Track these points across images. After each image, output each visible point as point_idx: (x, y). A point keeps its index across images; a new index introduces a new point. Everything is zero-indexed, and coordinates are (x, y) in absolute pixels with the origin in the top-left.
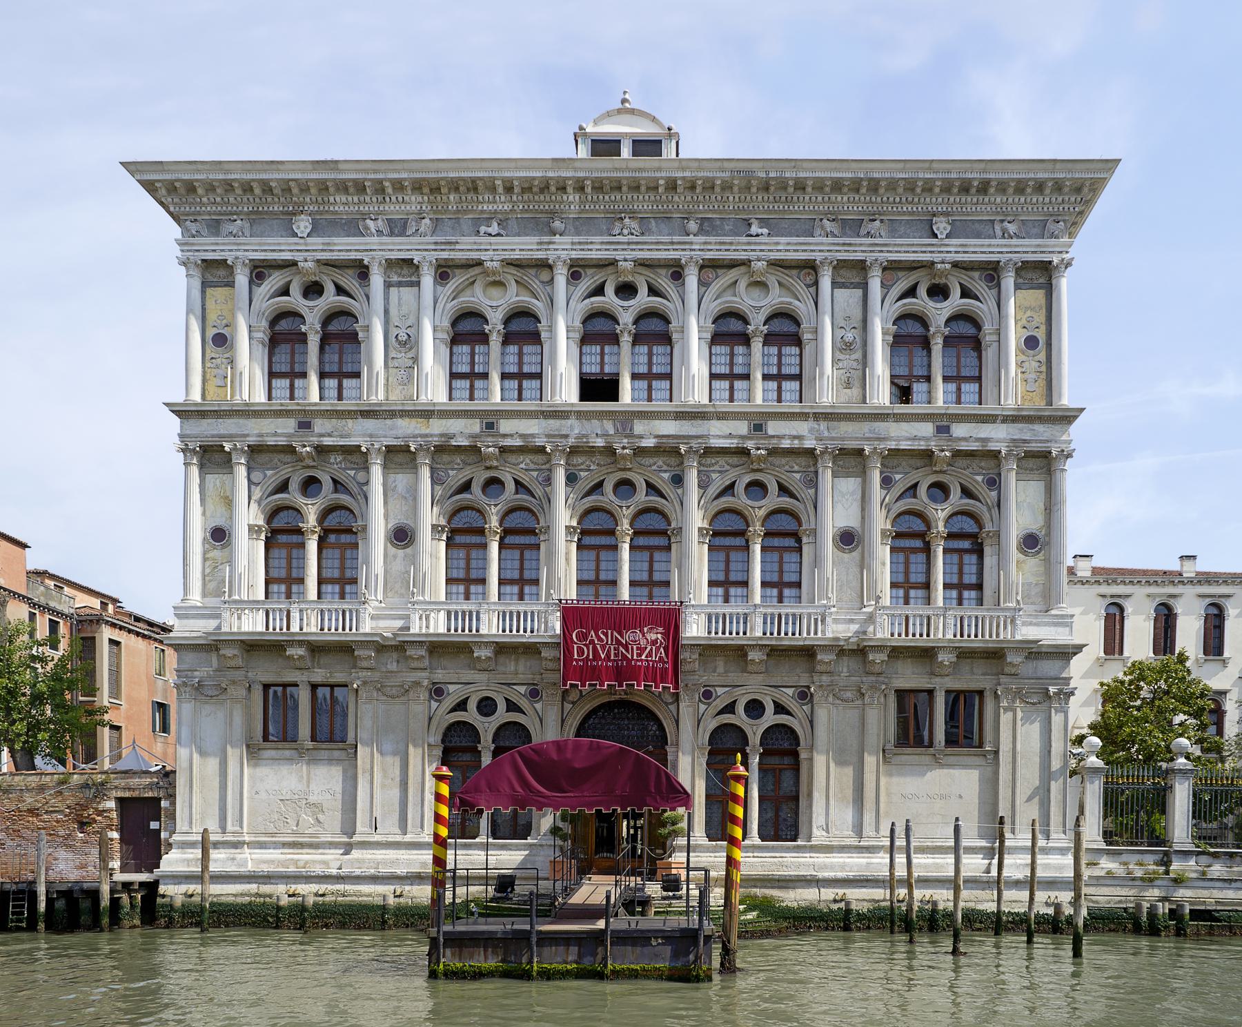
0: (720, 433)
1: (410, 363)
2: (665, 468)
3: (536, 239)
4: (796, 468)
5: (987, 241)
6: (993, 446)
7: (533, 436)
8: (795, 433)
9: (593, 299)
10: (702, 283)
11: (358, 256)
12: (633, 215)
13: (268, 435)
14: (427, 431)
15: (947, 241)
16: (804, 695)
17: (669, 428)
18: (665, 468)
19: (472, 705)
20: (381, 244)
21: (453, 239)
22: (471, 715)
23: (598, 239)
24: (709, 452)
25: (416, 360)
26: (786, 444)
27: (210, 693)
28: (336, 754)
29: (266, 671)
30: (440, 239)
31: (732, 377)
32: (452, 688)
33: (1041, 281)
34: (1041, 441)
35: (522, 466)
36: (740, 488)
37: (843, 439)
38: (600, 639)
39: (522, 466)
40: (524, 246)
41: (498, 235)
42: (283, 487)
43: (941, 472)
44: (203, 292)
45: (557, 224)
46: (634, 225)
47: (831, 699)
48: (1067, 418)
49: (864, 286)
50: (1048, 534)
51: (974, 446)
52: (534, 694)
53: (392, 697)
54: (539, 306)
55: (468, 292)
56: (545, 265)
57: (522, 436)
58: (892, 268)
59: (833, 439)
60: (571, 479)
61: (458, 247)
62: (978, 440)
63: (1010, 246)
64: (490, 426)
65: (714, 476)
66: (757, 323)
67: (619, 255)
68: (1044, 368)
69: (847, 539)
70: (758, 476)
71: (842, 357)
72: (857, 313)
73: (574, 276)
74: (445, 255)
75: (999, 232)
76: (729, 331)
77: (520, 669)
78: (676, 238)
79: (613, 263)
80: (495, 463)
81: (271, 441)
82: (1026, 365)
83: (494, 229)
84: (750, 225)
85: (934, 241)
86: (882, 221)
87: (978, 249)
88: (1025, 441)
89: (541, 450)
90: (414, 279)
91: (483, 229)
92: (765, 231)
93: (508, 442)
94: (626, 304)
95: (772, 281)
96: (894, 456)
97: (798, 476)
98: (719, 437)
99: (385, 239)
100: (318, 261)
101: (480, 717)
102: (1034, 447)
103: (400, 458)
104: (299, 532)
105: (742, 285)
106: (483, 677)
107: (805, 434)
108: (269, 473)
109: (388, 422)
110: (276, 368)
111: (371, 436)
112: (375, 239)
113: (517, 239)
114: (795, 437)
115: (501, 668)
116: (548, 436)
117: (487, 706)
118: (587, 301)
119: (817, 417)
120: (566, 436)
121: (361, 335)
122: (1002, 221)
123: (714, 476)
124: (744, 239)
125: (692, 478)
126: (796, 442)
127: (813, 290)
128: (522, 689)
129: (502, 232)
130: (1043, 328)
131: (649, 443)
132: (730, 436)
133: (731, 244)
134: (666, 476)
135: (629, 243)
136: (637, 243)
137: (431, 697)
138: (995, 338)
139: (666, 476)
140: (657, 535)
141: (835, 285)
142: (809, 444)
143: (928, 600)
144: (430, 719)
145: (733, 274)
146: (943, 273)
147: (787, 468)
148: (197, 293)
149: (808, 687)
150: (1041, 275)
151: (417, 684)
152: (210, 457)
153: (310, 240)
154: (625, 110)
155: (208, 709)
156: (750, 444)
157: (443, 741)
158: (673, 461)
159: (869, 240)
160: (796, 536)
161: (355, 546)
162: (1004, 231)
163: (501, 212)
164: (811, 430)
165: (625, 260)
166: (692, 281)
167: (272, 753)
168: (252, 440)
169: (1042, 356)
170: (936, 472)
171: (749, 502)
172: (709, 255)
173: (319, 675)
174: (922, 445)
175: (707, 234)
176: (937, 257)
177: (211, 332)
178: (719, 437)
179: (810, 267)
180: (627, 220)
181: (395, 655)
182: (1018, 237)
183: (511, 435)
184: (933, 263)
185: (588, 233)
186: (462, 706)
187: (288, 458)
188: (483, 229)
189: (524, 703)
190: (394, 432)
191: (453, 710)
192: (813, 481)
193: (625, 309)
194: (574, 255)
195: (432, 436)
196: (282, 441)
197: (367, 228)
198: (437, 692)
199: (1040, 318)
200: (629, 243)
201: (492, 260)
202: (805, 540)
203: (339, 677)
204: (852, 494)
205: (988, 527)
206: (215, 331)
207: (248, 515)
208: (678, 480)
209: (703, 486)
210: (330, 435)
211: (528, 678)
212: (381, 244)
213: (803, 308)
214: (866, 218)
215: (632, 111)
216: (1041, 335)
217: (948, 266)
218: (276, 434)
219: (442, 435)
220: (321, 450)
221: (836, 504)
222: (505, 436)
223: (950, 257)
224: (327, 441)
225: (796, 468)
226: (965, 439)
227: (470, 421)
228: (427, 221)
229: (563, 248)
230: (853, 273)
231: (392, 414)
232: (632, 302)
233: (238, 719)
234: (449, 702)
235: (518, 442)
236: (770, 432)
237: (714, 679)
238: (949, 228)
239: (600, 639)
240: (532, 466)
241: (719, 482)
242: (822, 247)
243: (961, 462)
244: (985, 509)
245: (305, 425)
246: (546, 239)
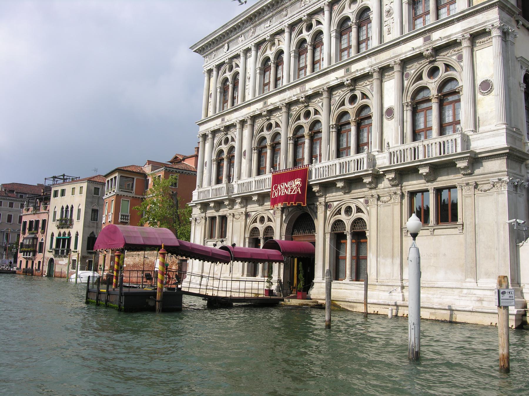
4: (368, 83)
6: (453, 38)
7: (276, 103)
8: (362, 67)
16: (367, 202)
34: (480, 24)
38: (281, 187)
51: (444, 42)
62: (445, 38)
88: (471, 28)
114: (361, 70)
116: (280, 101)
120: (285, 99)
126: (362, 71)
147: (364, 85)
168: (212, 129)
174: (417, 52)
219: (253, 112)
226: (438, 40)
239: (281, 187)
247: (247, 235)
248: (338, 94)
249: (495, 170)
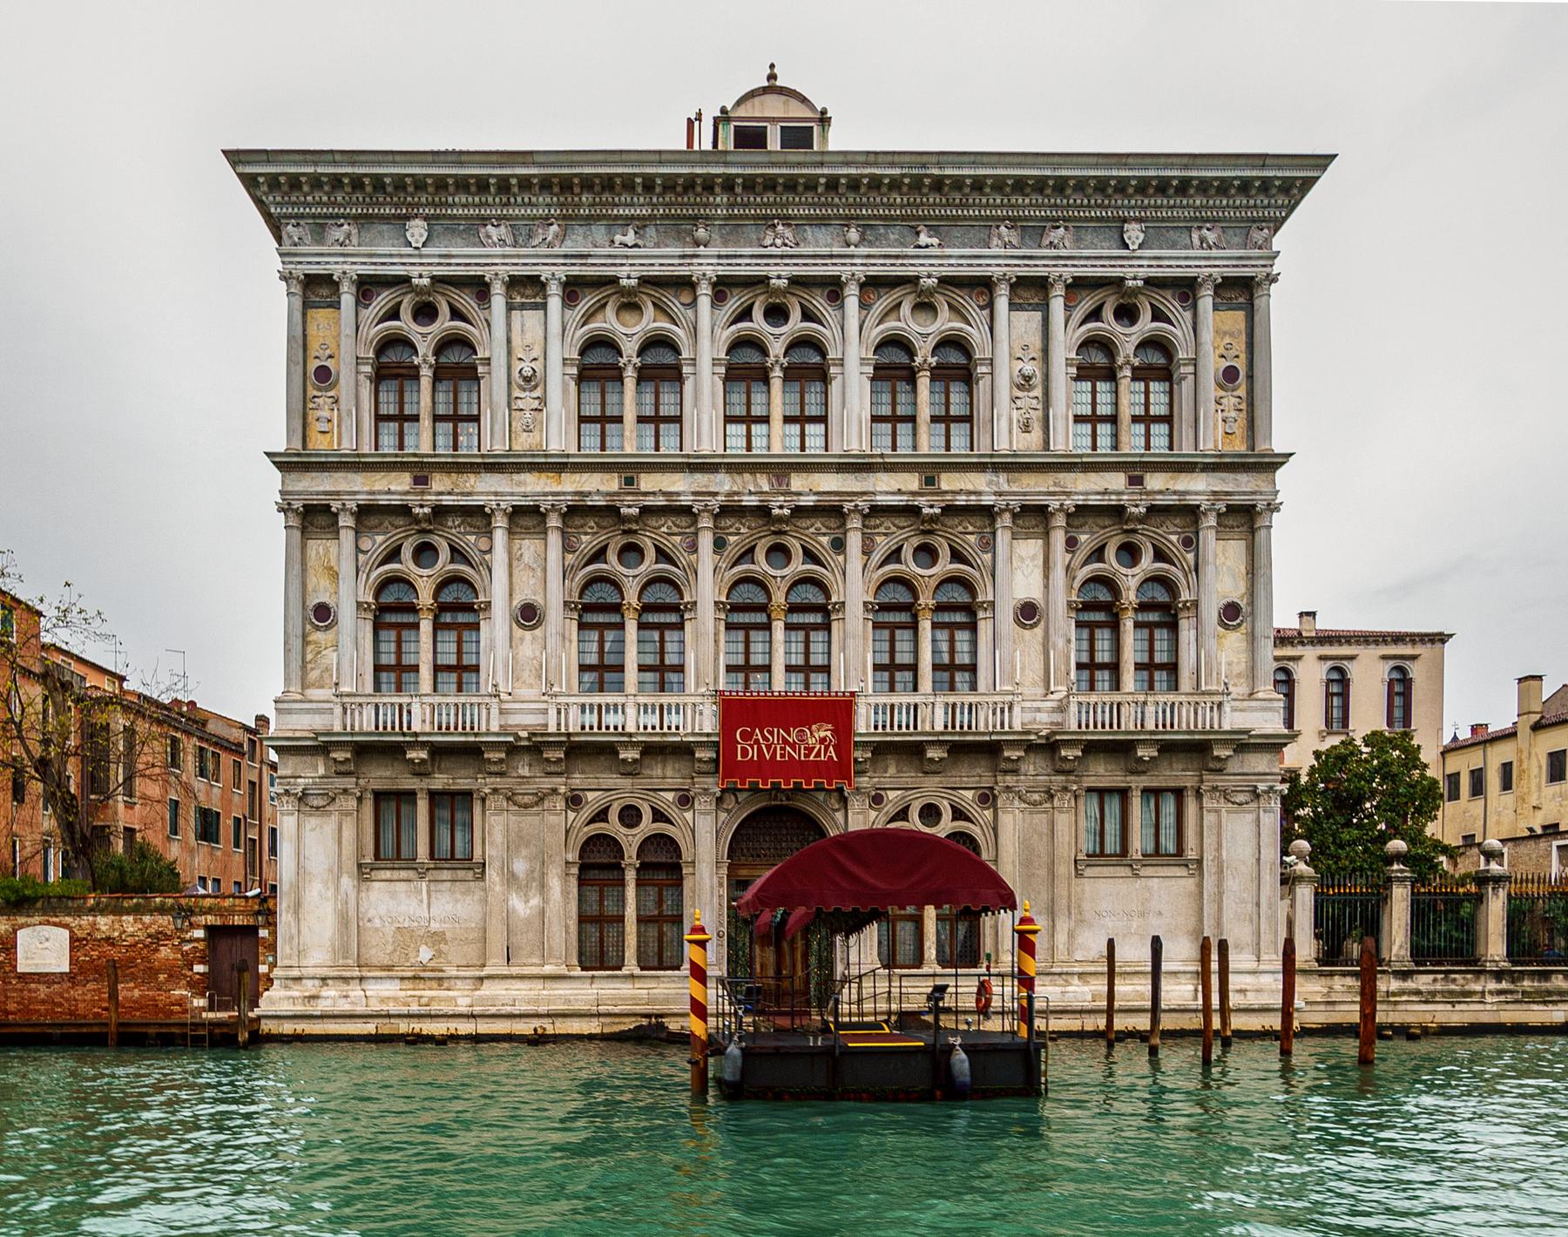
0: (887, 487)
1: (536, 404)
2: (824, 530)
3: (678, 251)
5: (1184, 253)
6: (1192, 500)
7: (678, 494)
8: (971, 487)
9: (740, 325)
10: (864, 306)
11: (478, 271)
12: (786, 220)
13: (380, 493)
14: (559, 489)
15: (1139, 253)
17: (830, 483)
18: (824, 530)
19: (613, 815)
20: (504, 256)
21: (584, 251)
22: (614, 827)
23: (748, 251)
24: (877, 511)
25: (543, 400)
26: (961, 500)
27: (315, 803)
28: (461, 874)
29: (381, 776)
30: (570, 251)
31: (894, 419)
32: (590, 796)
33: (1241, 300)
34: (1245, 493)
35: (664, 529)
36: (907, 552)
37: (1025, 494)
39: (664, 529)
40: (663, 257)
41: (636, 246)
42: (393, 555)
43: (1134, 531)
44: (304, 315)
45: (701, 233)
46: (788, 233)
47: (1016, 802)
48: (1270, 464)
49: (1045, 307)
50: (1252, 603)
52: (685, 801)
53: (526, 806)
54: (680, 334)
55: (600, 316)
56: (686, 284)
57: (665, 494)
58: (1078, 286)
59: (1014, 494)
60: (719, 544)
61: (590, 261)
63: (1208, 258)
64: (629, 481)
65: (878, 539)
66: (924, 354)
67: (772, 271)
68: (1243, 406)
69: (1028, 613)
70: (929, 540)
71: (1020, 394)
72: (1036, 341)
73: (719, 297)
74: (576, 271)
75: (1196, 241)
76: (894, 365)
77: (668, 775)
78: (836, 250)
79: (763, 281)
80: (634, 527)
81: (383, 500)
82: (1224, 401)
83: (630, 238)
84: (918, 233)
85: (1125, 253)
86: (1066, 228)
87: (1175, 261)
88: (1227, 493)
89: (686, 511)
90: (538, 300)
91: (618, 238)
92: (935, 241)
93: (650, 501)
94: (777, 331)
95: (941, 302)
96: (1082, 513)
97: (972, 538)
98: (887, 493)
99: (509, 250)
100: (433, 278)
101: (623, 830)
102: (1237, 500)
103: (527, 521)
104: (412, 609)
105: (906, 309)
106: (626, 783)
107: (981, 487)
108: (380, 539)
109: (515, 476)
110: (384, 411)
111: (496, 494)
112: (498, 250)
113: (656, 251)
114: (970, 493)
115: (647, 772)
116: (694, 494)
117: (630, 816)
118: (733, 328)
119: (997, 468)
121: (480, 369)
122: (1200, 228)
123: (878, 539)
124: (911, 251)
125: (854, 541)
127: (986, 312)
128: (670, 796)
129: (640, 242)
130: (1243, 356)
131: (808, 501)
132: (900, 492)
133: (897, 257)
134: (825, 540)
135: (782, 257)
136: (792, 257)
137: (568, 807)
138: (1191, 369)
139: (825, 540)
140: (816, 611)
141: (1013, 306)
142: (987, 500)
143: (1116, 685)
144: (567, 832)
145: (896, 294)
146: (1135, 292)
147: (960, 529)
148: (298, 316)
149: (992, 789)
150: (1243, 292)
151: (554, 791)
152: (312, 518)
153: (425, 251)
154: (772, 88)
155: (312, 821)
156: (921, 501)
157: (581, 857)
158: (833, 523)
159: (1053, 252)
160: (970, 609)
161: (476, 627)
162: (1202, 240)
163: (639, 218)
164: (990, 483)
165: (779, 277)
166: (852, 303)
167: (387, 874)
168: (363, 499)
169: (1242, 392)
170: (1126, 531)
171: (920, 571)
172: (873, 271)
173: (439, 782)
174: (1113, 500)
175: (871, 244)
176: (1129, 272)
177: (313, 365)
178: (887, 493)
179: (983, 286)
180: (780, 227)
181: (527, 759)
182: (1218, 247)
183: (654, 493)
184: (1122, 279)
185: (736, 244)
186: (601, 816)
187: (400, 521)
188: (618, 238)
189: (673, 813)
190: (522, 489)
191: (592, 821)
192: (989, 545)
193: (777, 337)
194: (721, 271)
195: (564, 494)
196: (395, 500)
197: (489, 237)
198: (574, 801)
199: (1240, 346)
200: (782, 257)
201: (628, 274)
202: (981, 614)
203: (463, 784)
204: (1033, 558)
205: (1185, 596)
206: (318, 363)
207: (349, 594)
208: (839, 545)
209: (867, 552)
210: (449, 494)
211: (677, 782)
212: (504, 256)
213: (976, 335)
214: (1049, 225)
215: (783, 91)
216: (1241, 365)
217: (1140, 283)
218: (389, 492)
219: (576, 493)
220: (440, 512)
221: (1021, 570)
222: (646, 494)
223: (1142, 272)
224: (447, 500)
225: (971, 529)
226: (1160, 492)
227: (607, 476)
228: (555, 228)
229: (706, 267)
230: (1031, 290)
231: (519, 468)
232: (783, 329)
233: (349, 833)
234: (586, 813)
235: (660, 501)
236: (944, 487)
237: (886, 782)
238: (1142, 236)
240: (675, 530)
241: (883, 545)
242: (999, 257)
243: (1157, 520)
244: (1180, 575)
245: (421, 481)
246: (689, 250)
247: (573, 856)
248: (882, 530)
249: (1260, 769)
